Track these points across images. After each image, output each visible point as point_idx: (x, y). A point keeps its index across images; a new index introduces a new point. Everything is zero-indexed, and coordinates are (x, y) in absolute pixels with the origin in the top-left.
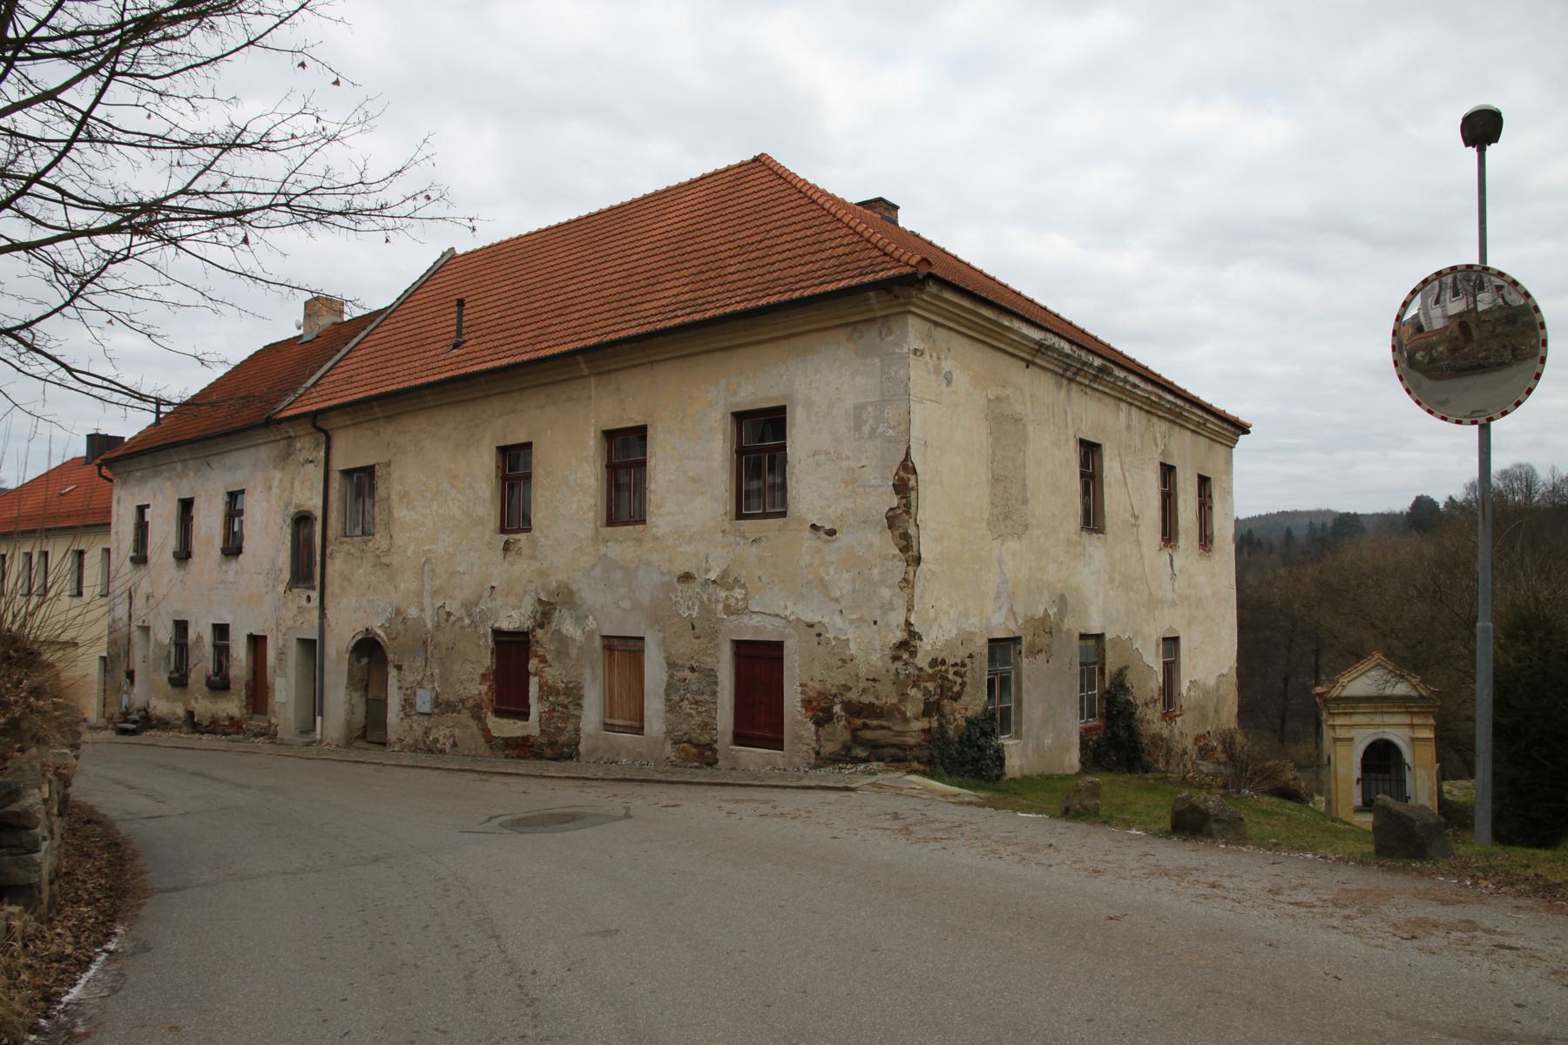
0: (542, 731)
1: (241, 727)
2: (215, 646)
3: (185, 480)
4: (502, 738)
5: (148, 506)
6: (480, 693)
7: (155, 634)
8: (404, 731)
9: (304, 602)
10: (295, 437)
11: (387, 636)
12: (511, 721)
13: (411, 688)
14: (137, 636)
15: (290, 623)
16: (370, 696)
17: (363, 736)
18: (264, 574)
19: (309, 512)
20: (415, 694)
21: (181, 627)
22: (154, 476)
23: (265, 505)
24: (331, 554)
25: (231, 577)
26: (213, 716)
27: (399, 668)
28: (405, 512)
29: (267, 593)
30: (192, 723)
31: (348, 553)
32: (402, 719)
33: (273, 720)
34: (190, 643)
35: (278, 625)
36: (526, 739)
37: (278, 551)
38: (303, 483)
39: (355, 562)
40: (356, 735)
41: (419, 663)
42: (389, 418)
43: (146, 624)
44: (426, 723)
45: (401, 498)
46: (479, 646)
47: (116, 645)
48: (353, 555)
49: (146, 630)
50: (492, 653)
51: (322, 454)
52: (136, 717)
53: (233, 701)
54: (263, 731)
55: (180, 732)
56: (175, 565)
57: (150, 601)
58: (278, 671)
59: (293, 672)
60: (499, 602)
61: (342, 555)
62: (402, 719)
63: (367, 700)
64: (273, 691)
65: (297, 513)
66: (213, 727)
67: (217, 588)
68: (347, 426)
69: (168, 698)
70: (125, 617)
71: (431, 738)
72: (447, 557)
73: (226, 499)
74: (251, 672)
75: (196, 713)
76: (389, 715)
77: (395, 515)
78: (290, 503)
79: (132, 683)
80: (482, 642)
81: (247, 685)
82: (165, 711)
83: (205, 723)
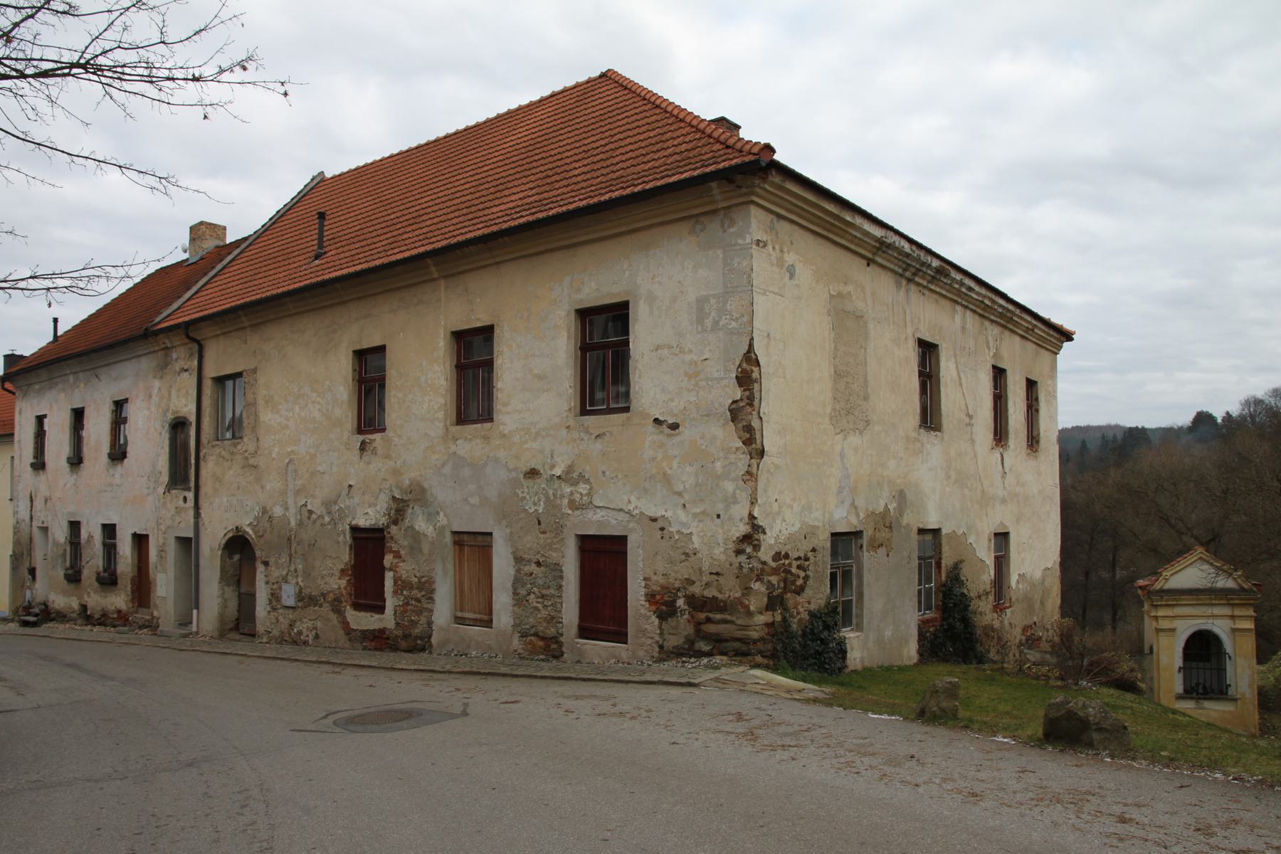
0: (397, 624)
1: (127, 620)
2: (104, 545)
3: (76, 390)
4: (360, 631)
5: (45, 416)
6: (339, 588)
7: (53, 534)
8: (271, 623)
9: (181, 503)
10: (172, 347)
11: (255, 533)
12: (368, 615)
13: (277, 582)
14: (37, 534)
15: (169, 523)
16: (243, 590)
17: (236, 628)
18: (146, 478)
19: (185, 418)
20: (280, 588)
21: (75, 526)
22: (50, 388)
23: (146, 412)
24: (204, 457)
25: (118, 480)
26: (103, 610)
27: (266, 564)
28: (270, 415)
29: (148, 495)
30: (86, 617)
31: (220, 456)
32: (269, 612)
33: (155, 613)
34: (82, 542)
35: (158, 524)
36: (382, 631)
37: (158, 455)
38: (179, 390)
39: (226, 464)
40: (228, 627)
41: (284, 559)
42: (255, 326)
43: (45, 525)
44: (291, 617)
45: (267, 402)
46: (339, 542)
47: (20, 544)
49: (45, 530)
50: (351, 549)
51: (196, 363)
52: (36, 610)
53: (120, 596)
54: (147, 623)
55: (75, 624)
56: (68, 470)
57: (48, 504)
58: (159, 567)
59: (173, 569)
60: (357, 500)
61: (214, 458)
62: (269, 612)
63: (240, 595)
64: (155, 586)
65: (174, 419)
66: (103, 620)
67: (106, 491)
68: (218, 336)
69: (65, 593)
70: (27, 518)
71: (295, 630)
72: (308, 457)
73: (113, 407)
74: (136, 569)
75: (89, 606)
76: (257, 608)
77: (262, 419)
78: (168, 410)
79: (34, 578)
80: (341, 538)
81: (133, 580)
82: (62, 605)
83: (97, 616)
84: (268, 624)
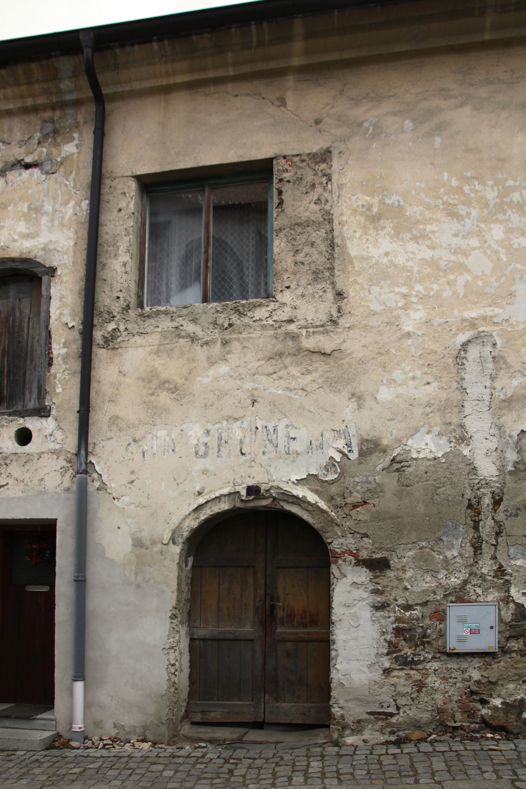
11: (330, 499)
13: (425, 604)
32: (387, 672)
39: (201, 352)
44: (476, 675)
48: (193, 338)
61: (154, 339)
62: (387, 672)
71: (497, 702)
84: (387, 698)
